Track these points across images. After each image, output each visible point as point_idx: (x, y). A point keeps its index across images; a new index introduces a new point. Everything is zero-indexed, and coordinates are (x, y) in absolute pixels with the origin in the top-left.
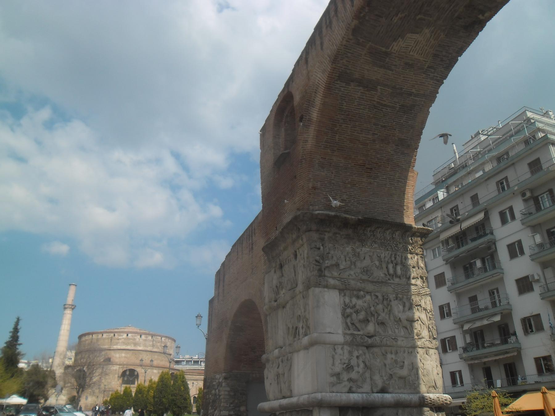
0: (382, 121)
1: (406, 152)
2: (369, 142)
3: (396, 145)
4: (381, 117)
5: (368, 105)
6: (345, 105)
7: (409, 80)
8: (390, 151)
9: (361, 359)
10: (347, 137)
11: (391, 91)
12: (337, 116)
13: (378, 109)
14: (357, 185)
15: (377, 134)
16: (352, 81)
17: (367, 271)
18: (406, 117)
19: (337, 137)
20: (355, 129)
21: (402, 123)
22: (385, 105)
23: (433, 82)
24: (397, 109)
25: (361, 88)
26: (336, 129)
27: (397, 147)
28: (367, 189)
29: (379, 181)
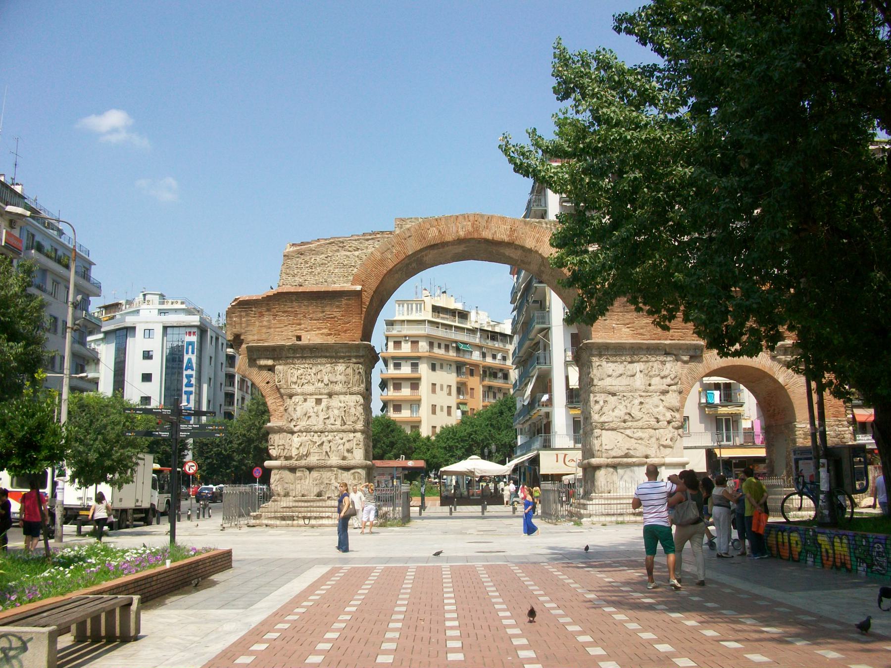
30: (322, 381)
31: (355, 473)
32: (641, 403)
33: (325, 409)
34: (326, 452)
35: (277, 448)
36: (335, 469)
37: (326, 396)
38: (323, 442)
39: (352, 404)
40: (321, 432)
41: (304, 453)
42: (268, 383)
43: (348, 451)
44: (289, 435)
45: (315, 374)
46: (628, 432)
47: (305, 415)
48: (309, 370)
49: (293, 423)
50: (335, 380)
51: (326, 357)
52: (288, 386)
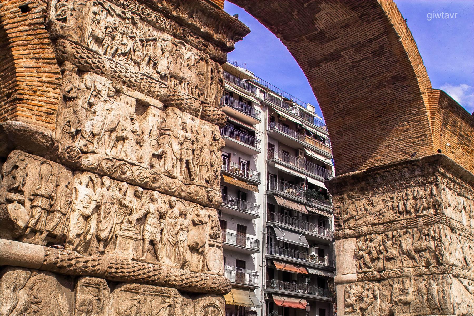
0: (367, 72)
1: (405, 85)
2: (368, 94)
3: (393, 84)
4: (364, 70)
5: (347, 69)
6: (330, 80)
7: (358, 34)
8: (390, 92)
9: (370, 291)
10: (348, 101)
11: (353, 49)
12: (331, 90)
13: (357, 67)
14: (373, 136)
15: (371, 85)
16: (320, 63)
17: (380, 214)
18: (384, 58)
19: (341, 106)
20: (351, 91)
21: (385, 64)
22: (359, 61)
23: (378, 22)
24: (371, 57)
25: (330, 62)
26: (337, 100)
27: (394, 85)
28: (381, 136)
29: (391, 123)
30: (155, 65)
31: (208, 306)
32: (470, 247)
33: (156, 132)
34: (152, 242)
35: (28, 203)
36: (173, 291)
37: (160, 105)
38: (146, 215)
39: (208, 140)
40: (144, 189)
41: (103, 235)
42: (25, 9)
43: (194, 249)
44: (65, 172)
45: (142, 41)
46: (466, 282)
47: (112, 130)
48: (131, 27)
49: (79, 144)
50: (181, 75)
51: (167, 14)
52: (82, 39)
